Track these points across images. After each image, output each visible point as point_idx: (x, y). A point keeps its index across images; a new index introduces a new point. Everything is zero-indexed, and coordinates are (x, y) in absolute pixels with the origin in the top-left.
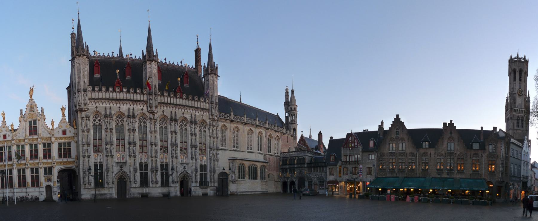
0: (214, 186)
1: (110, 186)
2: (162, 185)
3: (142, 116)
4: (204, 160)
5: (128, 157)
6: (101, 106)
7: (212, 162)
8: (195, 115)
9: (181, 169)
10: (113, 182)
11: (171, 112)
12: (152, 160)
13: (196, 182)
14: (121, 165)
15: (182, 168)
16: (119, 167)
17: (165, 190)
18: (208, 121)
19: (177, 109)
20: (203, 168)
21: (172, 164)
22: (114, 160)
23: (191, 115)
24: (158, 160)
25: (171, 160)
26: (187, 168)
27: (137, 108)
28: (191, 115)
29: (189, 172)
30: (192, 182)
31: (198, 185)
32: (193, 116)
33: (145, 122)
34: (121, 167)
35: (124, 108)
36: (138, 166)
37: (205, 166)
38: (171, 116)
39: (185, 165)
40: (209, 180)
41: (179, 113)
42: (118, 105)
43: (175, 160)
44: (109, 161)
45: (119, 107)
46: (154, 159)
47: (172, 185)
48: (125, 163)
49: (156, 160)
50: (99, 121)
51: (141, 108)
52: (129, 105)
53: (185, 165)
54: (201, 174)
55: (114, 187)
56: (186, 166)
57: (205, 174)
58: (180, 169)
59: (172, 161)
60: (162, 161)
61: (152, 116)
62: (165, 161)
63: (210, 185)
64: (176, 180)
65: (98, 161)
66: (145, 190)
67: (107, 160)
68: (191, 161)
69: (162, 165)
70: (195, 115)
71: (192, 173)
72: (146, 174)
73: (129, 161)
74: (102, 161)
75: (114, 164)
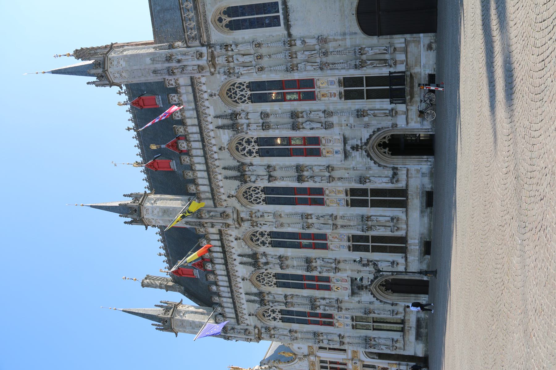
0: (405, 51)
1: (401, 310)
2: (403, 205)
3: (252, 240)
4: (328, 84)
5: (339, 275)
6: (246, 307)
7: (330, 59)
8: (217, 117)
9: (359, 159)
10: (392, 305)
11: (226, 178)
12: (342, 226)
13: (393, 113)
14: (357, 287)
15: (356, 154)
16: (362, 293)
17: (415, 202)
18: (221, 78)
19: (217, 163)
20: (352, 88)
21: (349, 179)
22: (347, 298)
23: (218, 127)
24: (341, 213)
25: (339, 184)
26: (355, 142)
27: (236, 247)
28: (218, 127)
29: (366, 134)
30: (395, 125)
31: (401, 107)
32: (220, 122)
33: (262, 234)
34: (361, 288)
35: (242, 271)
36: (357, 255)
37: (347, 82)
38: (235, 178)
39: (348, 148)
40: (384, 71)
41: (223, 160)
42: (239, 280)
43: (336, 174)
44: (351, 306)
45: (243, 280)
46: (339, 222)
47: (401, 185)
48: (353, 280)
49: (342, 217)
50: (273, 311)
51: (234, 240)
52: (236, 263)
53: (348, 148)
54: (371, 95)
55: (403, 304)
56: (351, 143)
57: (371, 81)
58: (359, 160)
59: (340, 179)
60: (344, 203)
61: (246, 225)
62: (343, 196)
63: (401, 68)
64: (390, 173)
65: (349, 322)
66: (414, 244)
67: (347, 309)
68: (336, 130)
69: (354, 204)
70: (217, 117)
71: (367, 126)
72: (375, 239)
73: (349, 273)
74: (349, 316)
75: (356, 299)
